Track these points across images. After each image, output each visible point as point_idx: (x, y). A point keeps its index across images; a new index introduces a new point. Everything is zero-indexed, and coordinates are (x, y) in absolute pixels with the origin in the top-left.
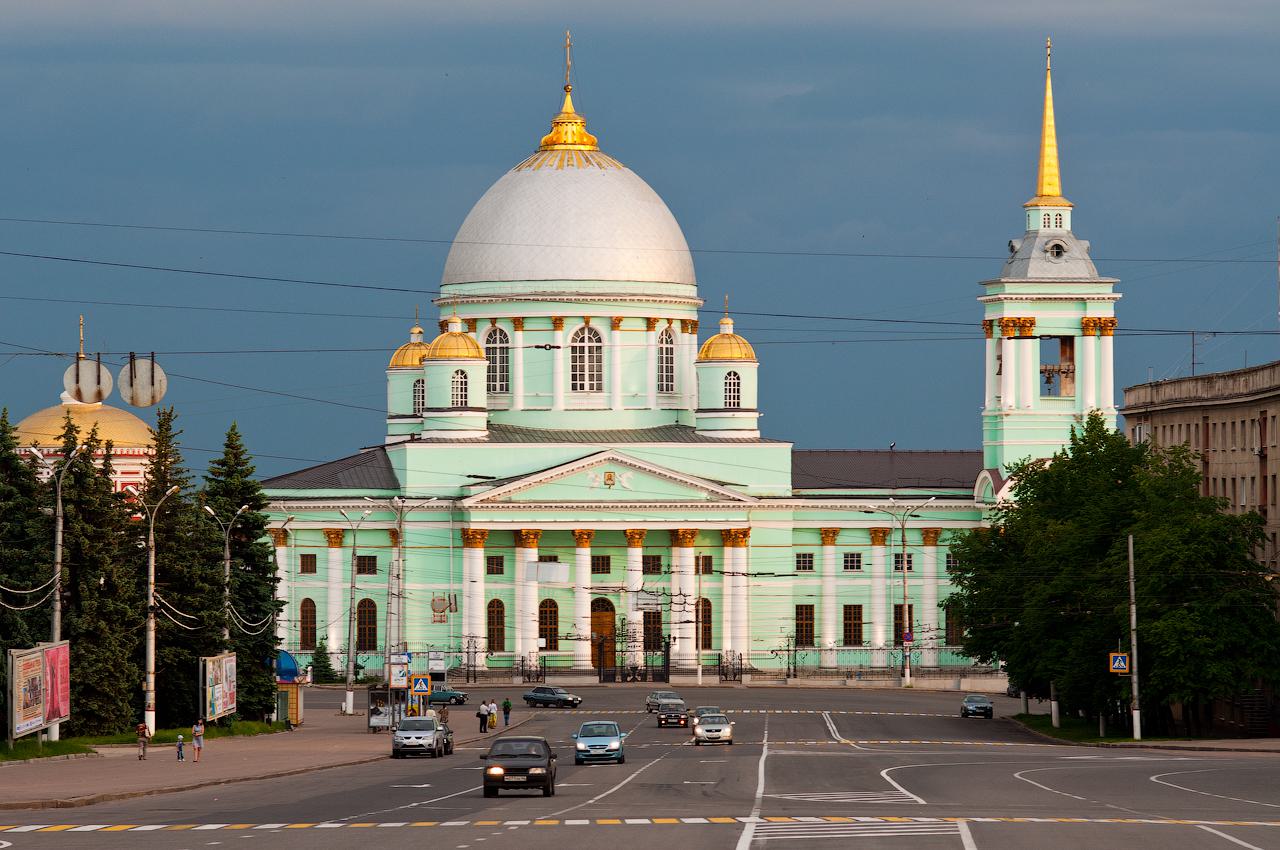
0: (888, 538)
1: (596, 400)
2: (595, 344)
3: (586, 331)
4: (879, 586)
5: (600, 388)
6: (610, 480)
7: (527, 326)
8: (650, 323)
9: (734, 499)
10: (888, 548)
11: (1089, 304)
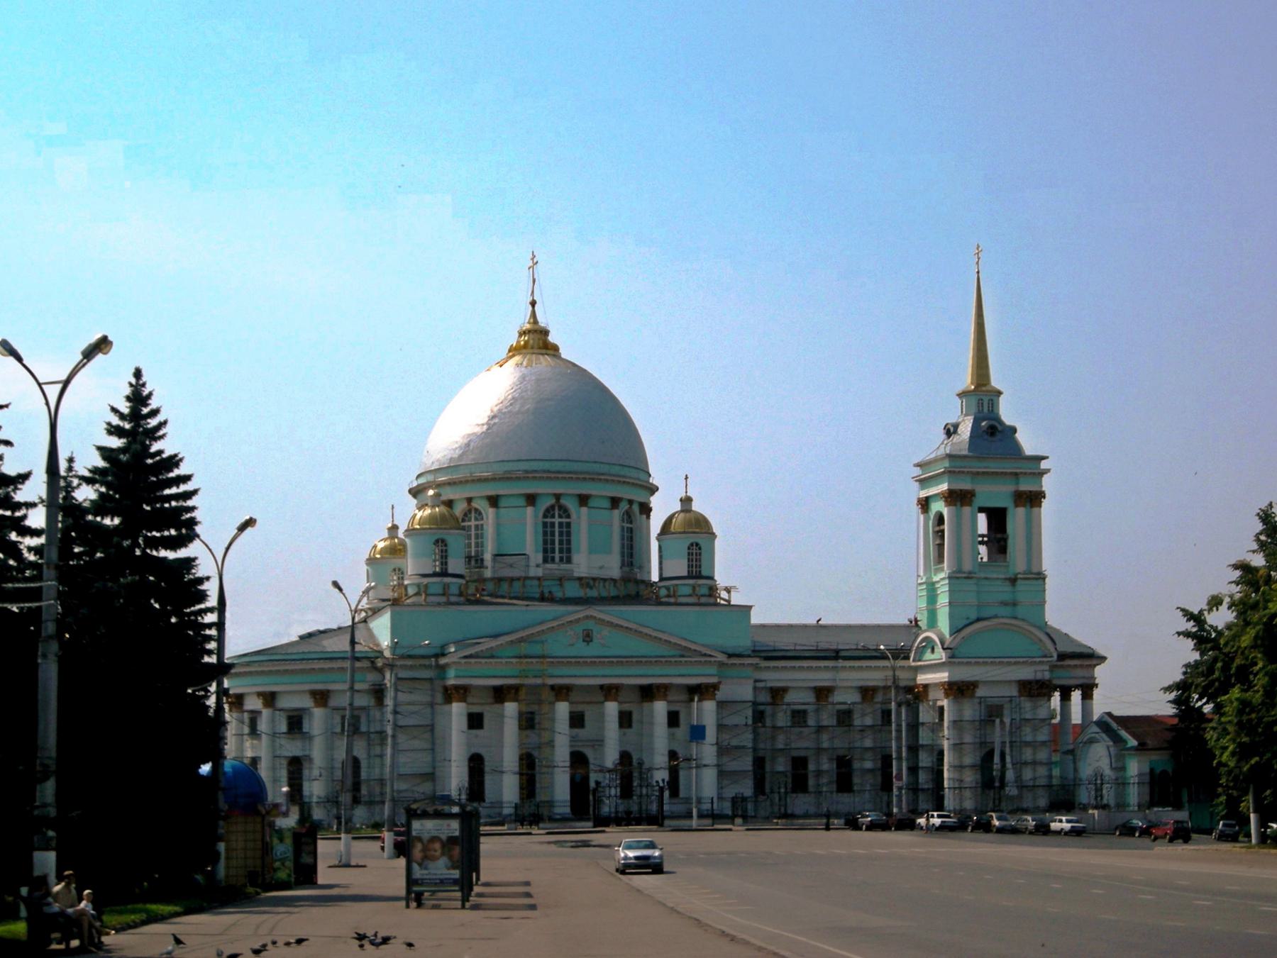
2: (564, 520)
6: (588, 637)
7: (502, 503)
8: (615, 502)
9: (705, 655)
11: (1022, 479)
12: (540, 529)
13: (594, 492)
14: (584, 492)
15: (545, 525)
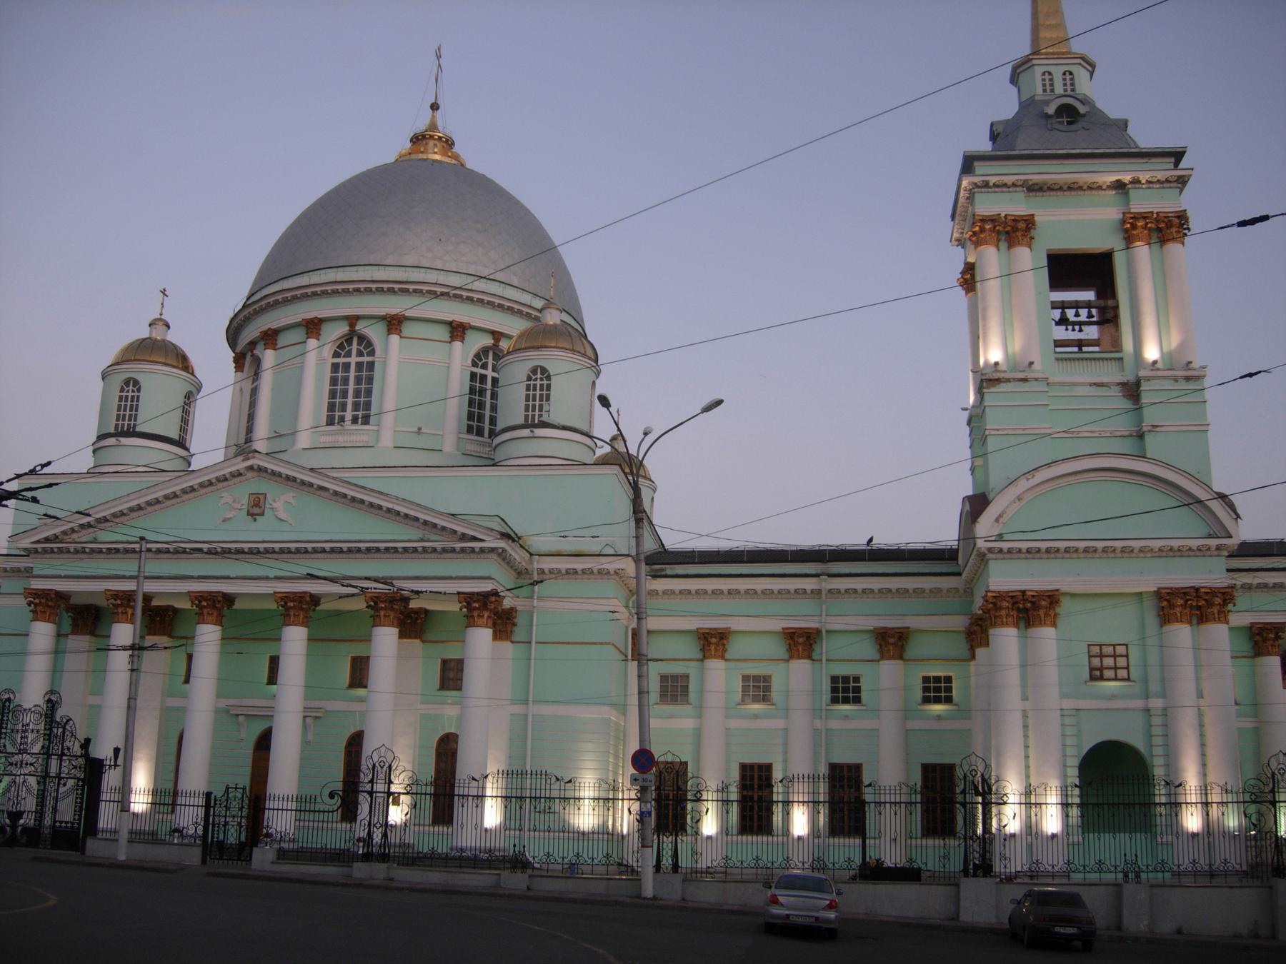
0: (816, 648)
1: (360, 433)
2: (365, 359)
3: (355, 341)
4: (800, 724)
5: (366, 420)
6: (257, 507)
9: (464, 537)
10: (817, 665)
12: (328, 374)
14: (393, 311)
15: (335, 367)
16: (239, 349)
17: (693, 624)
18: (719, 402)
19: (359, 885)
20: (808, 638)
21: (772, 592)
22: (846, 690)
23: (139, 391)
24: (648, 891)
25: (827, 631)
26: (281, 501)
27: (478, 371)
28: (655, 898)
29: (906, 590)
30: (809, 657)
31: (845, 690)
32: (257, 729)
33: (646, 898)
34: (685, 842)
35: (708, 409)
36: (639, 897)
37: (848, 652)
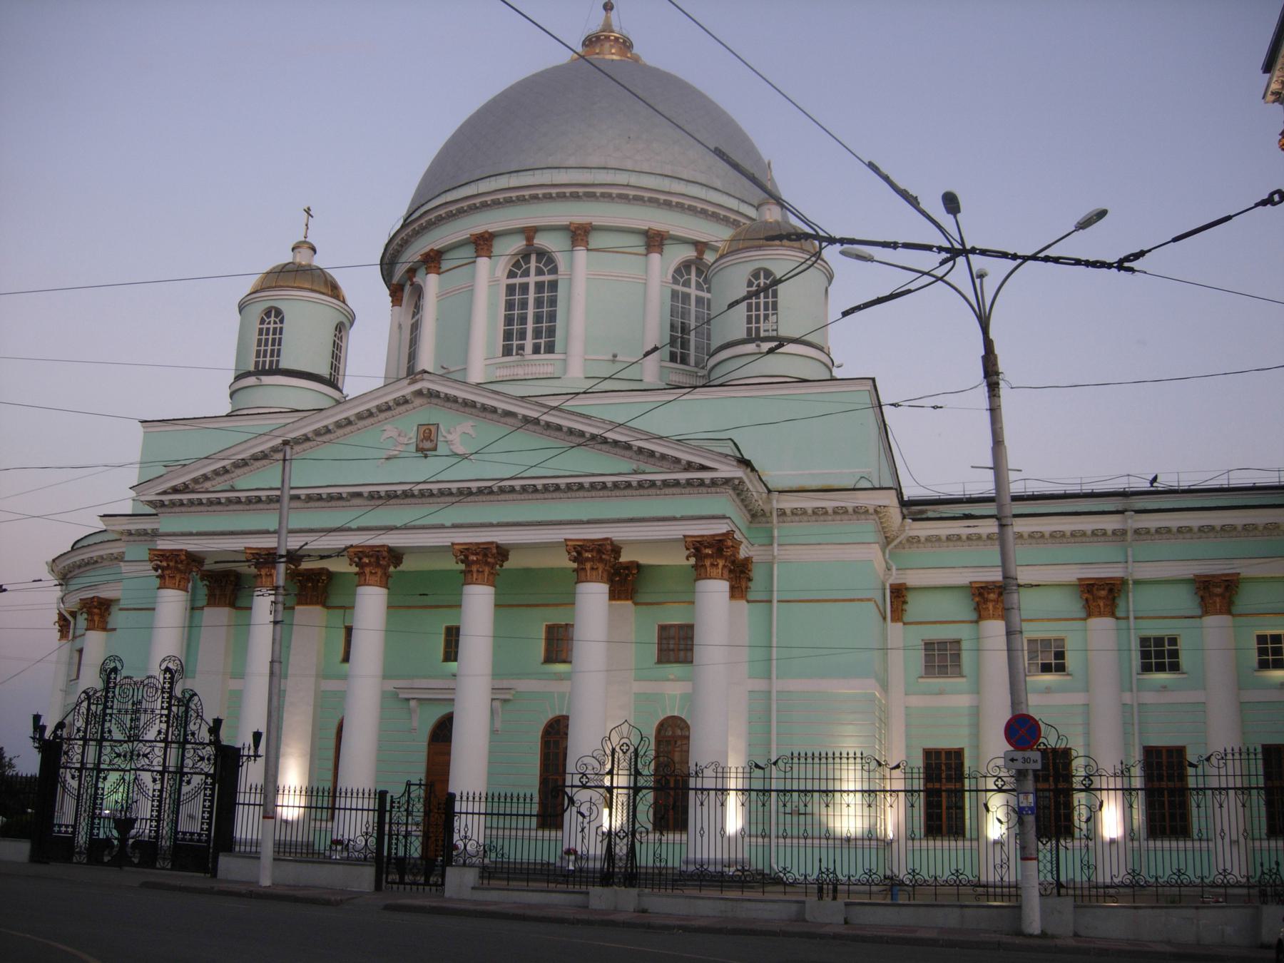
0: (1121, 603)
1: (544, 364)
2: (547, 278)
3: (533, 258)
4: (1106, 700)
5: (550, 349)
6: (427, 443)
9: (689, 466)
10: (1123, 623)
13: (596, 222)
15: (510, 289)
16: (395, 280)
17: (964, 578)
18: (1102, 214)
19: (607, 923)
20: (1111, 591)
21: (1063, 534)
22: (1160, 654)
23: (282, 321)
24: (1034, 921)
25: (1136, 582)
26: (458, 432)
27: (679, 288)
28: (1044, 935)
29: (1233, 528)
30: (1113, 615)
31: (1159, 655)
32: (432, 716)
33: (1031, 936)
34: (1071, 850)
35: (1084, 224)
36: (1020, 933)
37: (1159, 609)
